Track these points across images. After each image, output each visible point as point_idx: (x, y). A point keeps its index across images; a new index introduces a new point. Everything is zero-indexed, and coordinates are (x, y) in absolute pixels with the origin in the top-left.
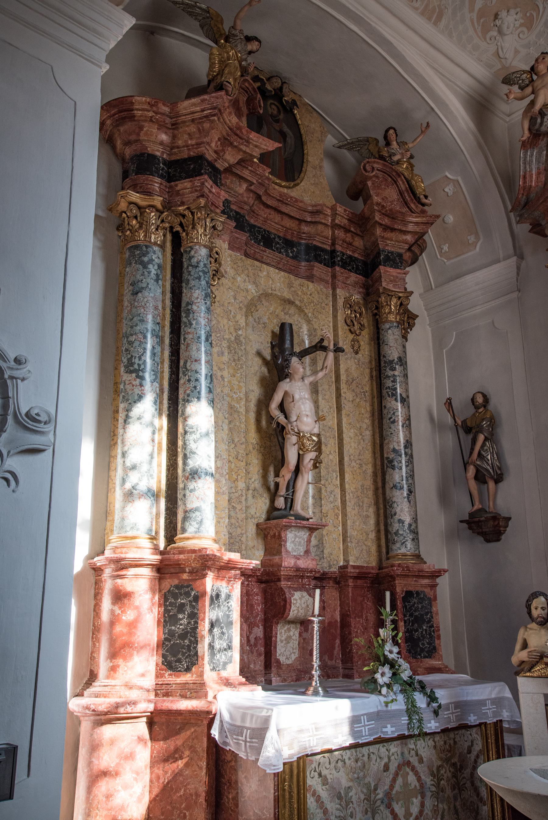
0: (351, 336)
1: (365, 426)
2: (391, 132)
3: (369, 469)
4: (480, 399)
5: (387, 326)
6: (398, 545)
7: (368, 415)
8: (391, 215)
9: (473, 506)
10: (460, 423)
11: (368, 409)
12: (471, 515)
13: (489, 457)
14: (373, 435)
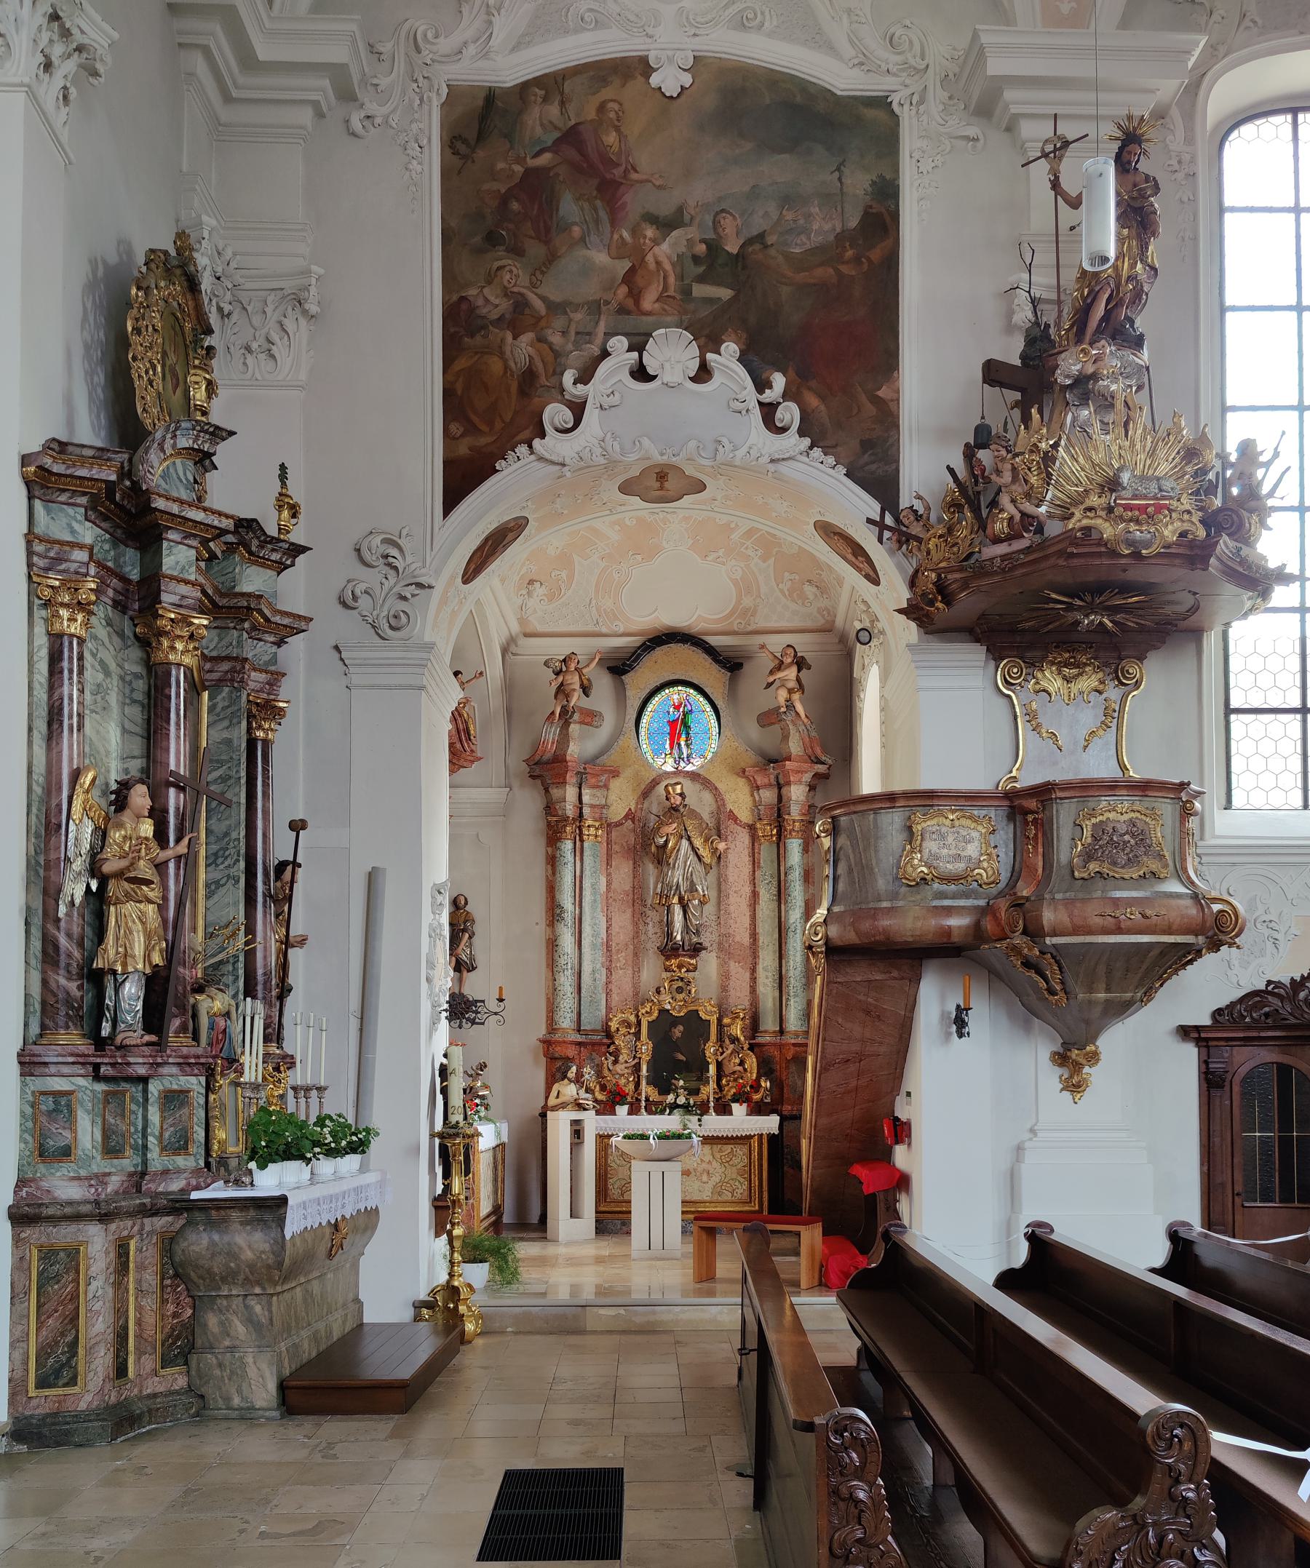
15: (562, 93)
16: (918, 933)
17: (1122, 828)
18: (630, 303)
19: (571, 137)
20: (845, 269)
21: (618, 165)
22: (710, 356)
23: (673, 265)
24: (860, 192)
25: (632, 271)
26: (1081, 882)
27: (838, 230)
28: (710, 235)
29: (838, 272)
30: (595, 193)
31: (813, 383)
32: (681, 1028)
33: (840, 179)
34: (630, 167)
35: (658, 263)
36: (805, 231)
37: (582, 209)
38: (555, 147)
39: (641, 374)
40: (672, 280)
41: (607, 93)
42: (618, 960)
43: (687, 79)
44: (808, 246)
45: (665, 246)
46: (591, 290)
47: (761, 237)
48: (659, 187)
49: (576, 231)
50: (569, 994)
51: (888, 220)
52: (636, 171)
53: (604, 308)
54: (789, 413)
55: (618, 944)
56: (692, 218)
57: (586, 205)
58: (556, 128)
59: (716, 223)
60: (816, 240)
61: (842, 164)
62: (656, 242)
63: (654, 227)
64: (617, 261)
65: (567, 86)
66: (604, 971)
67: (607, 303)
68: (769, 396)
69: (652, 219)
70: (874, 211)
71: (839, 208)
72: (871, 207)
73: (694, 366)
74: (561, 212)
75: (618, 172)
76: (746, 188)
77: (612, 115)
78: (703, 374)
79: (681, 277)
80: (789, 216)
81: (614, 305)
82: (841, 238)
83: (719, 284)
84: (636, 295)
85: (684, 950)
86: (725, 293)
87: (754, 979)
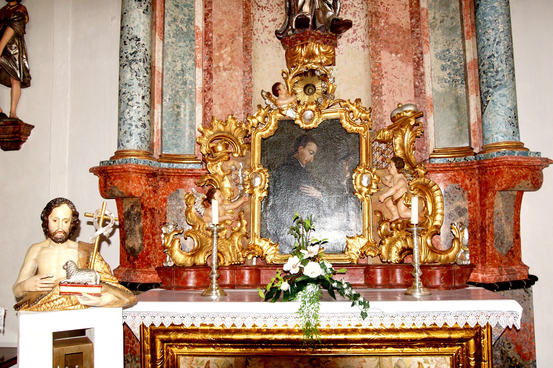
32: (313, 147)
42: (221, 57)
50: (139, 99)
55: (220, 36)
66: (199, 73)
85: (314, 27)
87: (419, 76)
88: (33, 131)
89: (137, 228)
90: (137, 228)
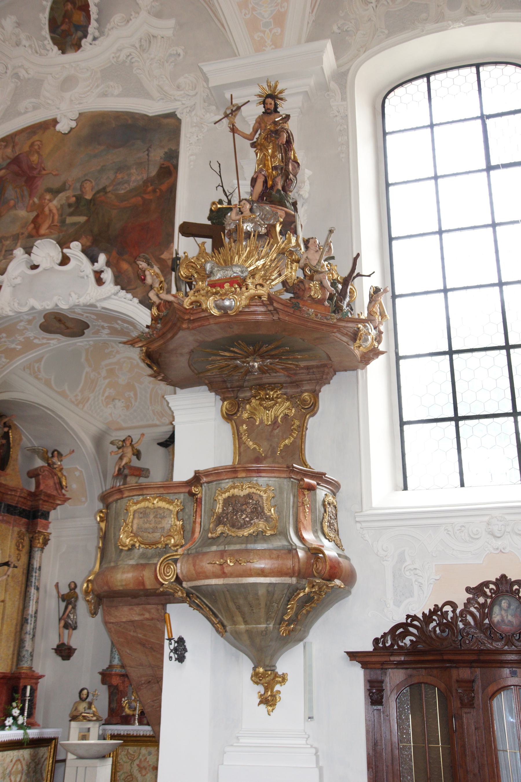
0: (17, 552)
1: (16, 599)
2: (56, 453)
3: (14, 622)
4: (73, 586)
5: (36, 549)
6: (24, 662)
7: (18, 593)
8: (49, 496)
9: (60, 641)
10: (60, 596)
11: (19, 589)
12: (58, 646)
13: (72, 617)
14: (19, 604)
15: (14, 142)
16: (124, 583)
17: (242, 500)
18: (34, 232)
19: (16, 161)
20: (147, 197)
21: (36, 169)
22: (65, 251)
23: (58, 210)
24: (158, 159)
25: (37, 216)
26: (210, 540)
27: (145, 178)
28: (78, 192)
29: (142, 198)
30: (23, 183)
31: (126, 257)
33: (148, 155)
34: (42, 169)
35: (50, 211)
36: (127, 182)
37: (16, 192)
38: (7, 167)
39: (34, 267)
40: (56, 217)
41: (36, 138)
43: (73, 124)
44: (128, 189)
45: (55, 202)
46: (15, 229)
47: (104, 189)
48: (56, 175)
49: (12, 203)
51: (172, 168)
52: (44, 170)
53: (20, 236)
54: (108, 275)
56: (70, 186)
57: (18, 190)
58: (9, 158)
59: (82, 186)
60: (133, 185)
61: (150, 147)
62: (50, 201)
63: (51, 194)
64: (30, 213)
65: (17, 139)
67: (22, 234)
68: (97, 266)
69: (49, 190)
70: (165, 166)
71: (147, 168)
72: (163, 164)
73: (60, 257)
74: (6, 195)
75: (35, 172)
76: (99, 168)
77: (36, 147)
78: (65, 261)
79: (61, 215)
80: (120, 176)
81: (26, 234)
82: (146, 182)
83: (80, 215)
84: (37, 228)
86: (82, 219)
88: (76, 652)
89: (115, 699)
90: (115, 699)
